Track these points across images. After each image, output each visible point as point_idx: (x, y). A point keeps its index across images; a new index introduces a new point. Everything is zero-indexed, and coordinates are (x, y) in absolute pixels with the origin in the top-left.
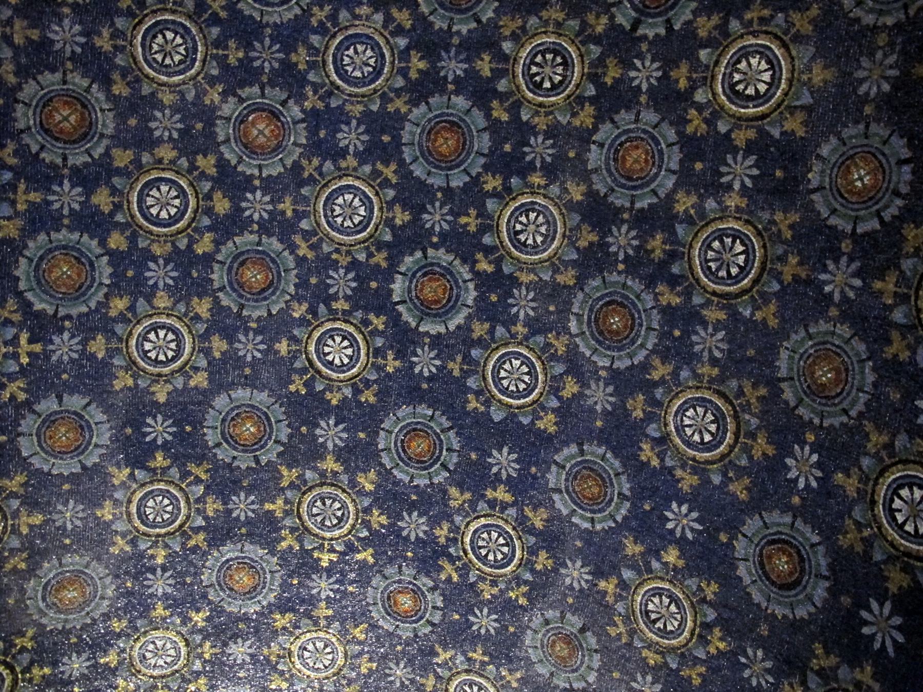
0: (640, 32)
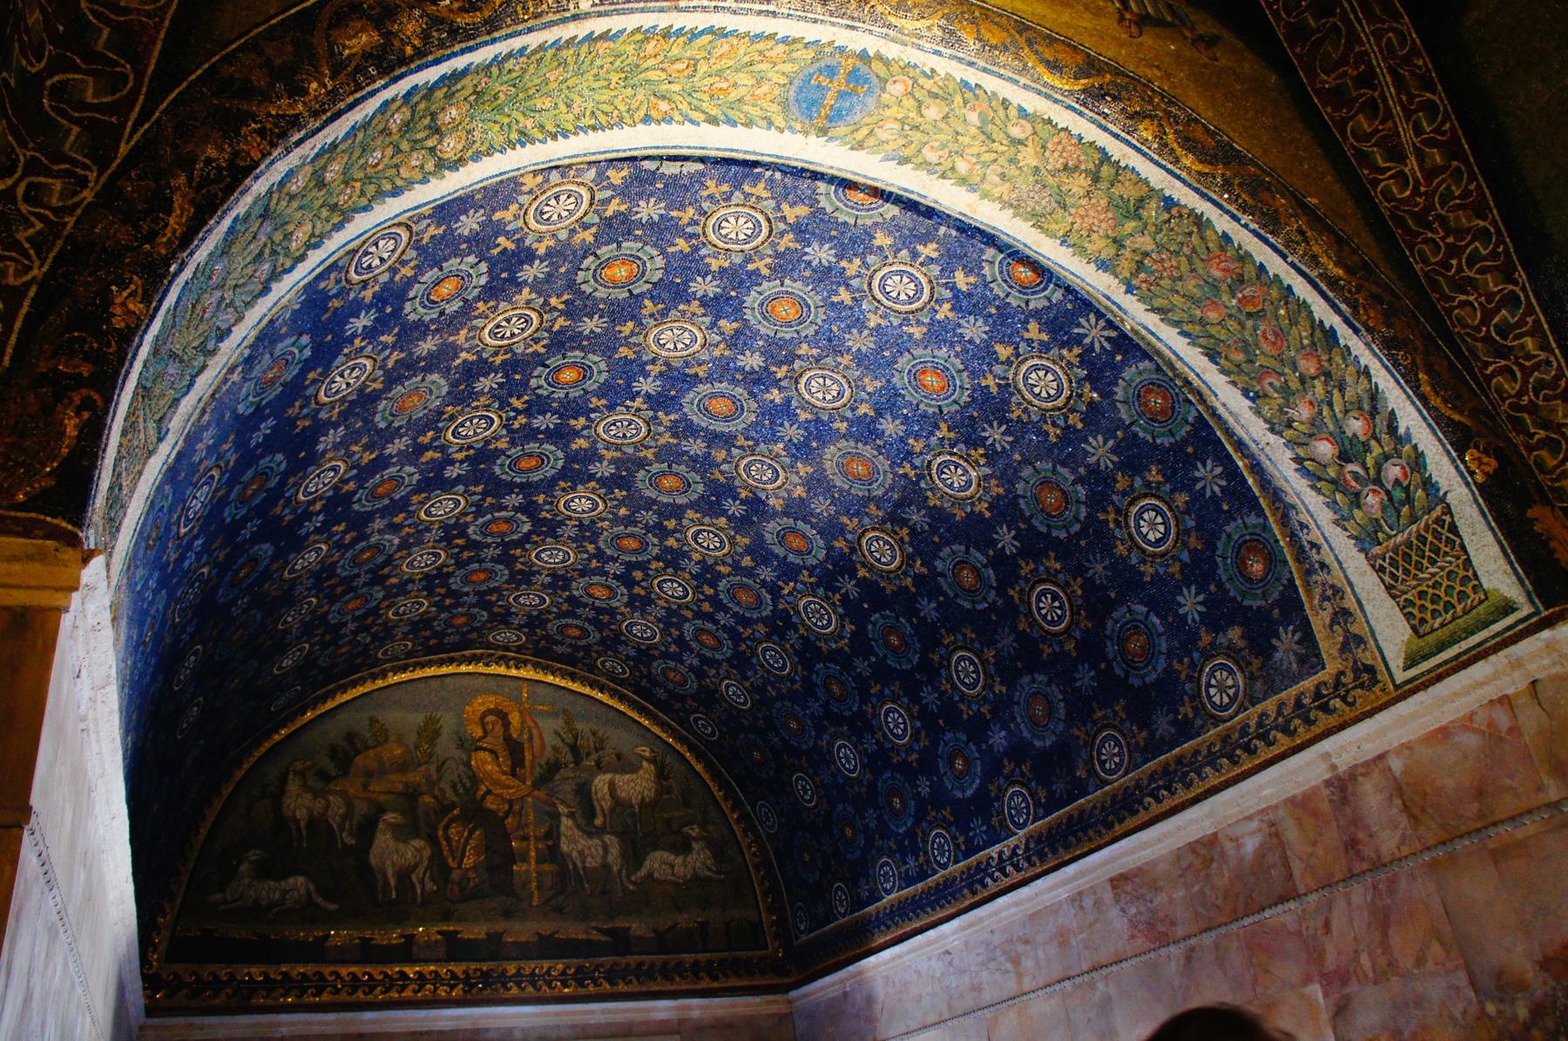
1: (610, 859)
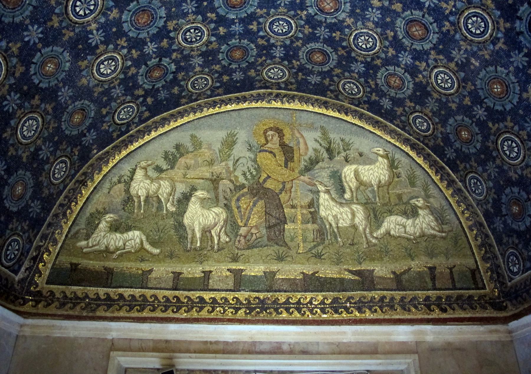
0: (158, 59)
1: (357, 221)
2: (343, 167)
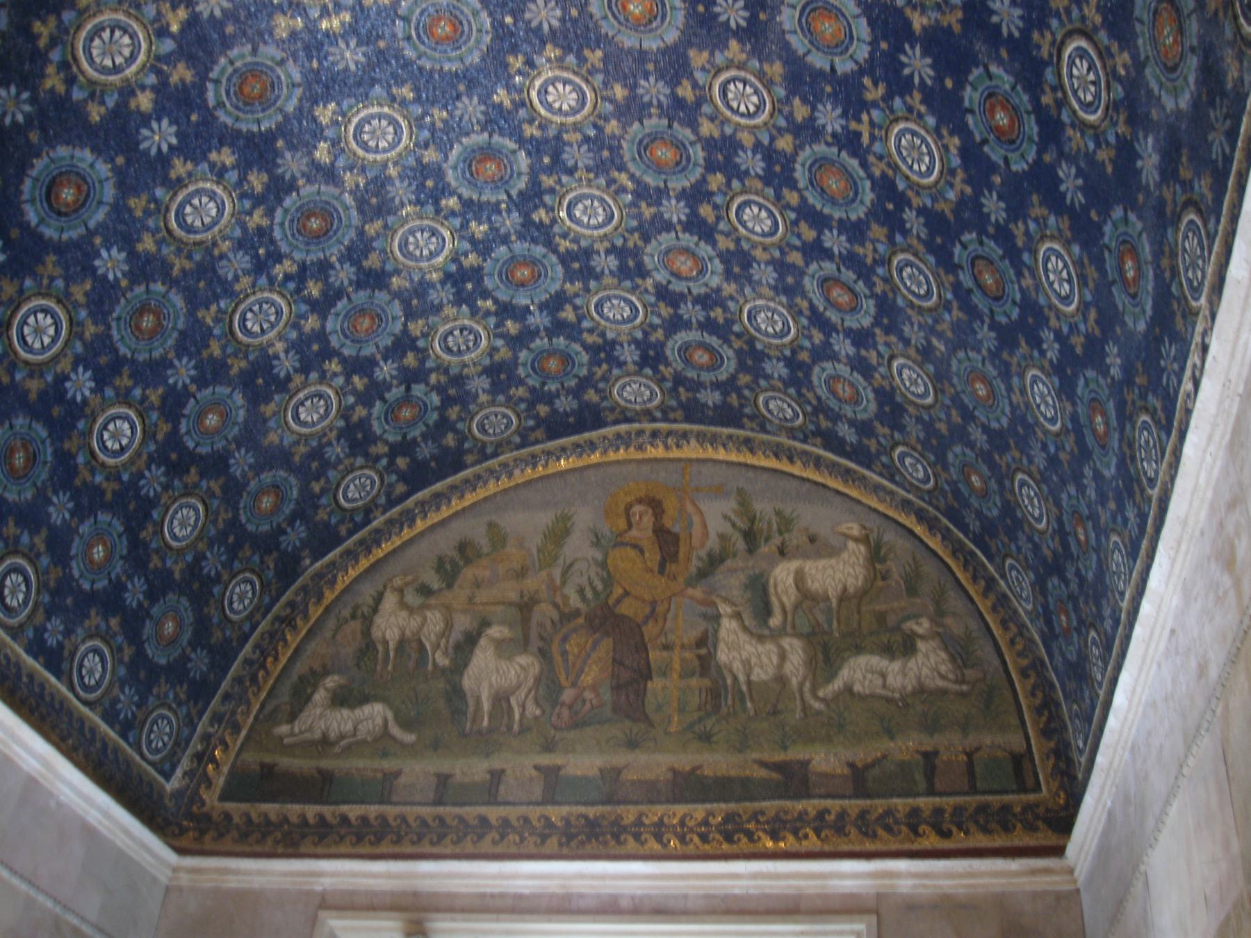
0: (403, 388)
1: (788, 668)
2: (773, 565)
